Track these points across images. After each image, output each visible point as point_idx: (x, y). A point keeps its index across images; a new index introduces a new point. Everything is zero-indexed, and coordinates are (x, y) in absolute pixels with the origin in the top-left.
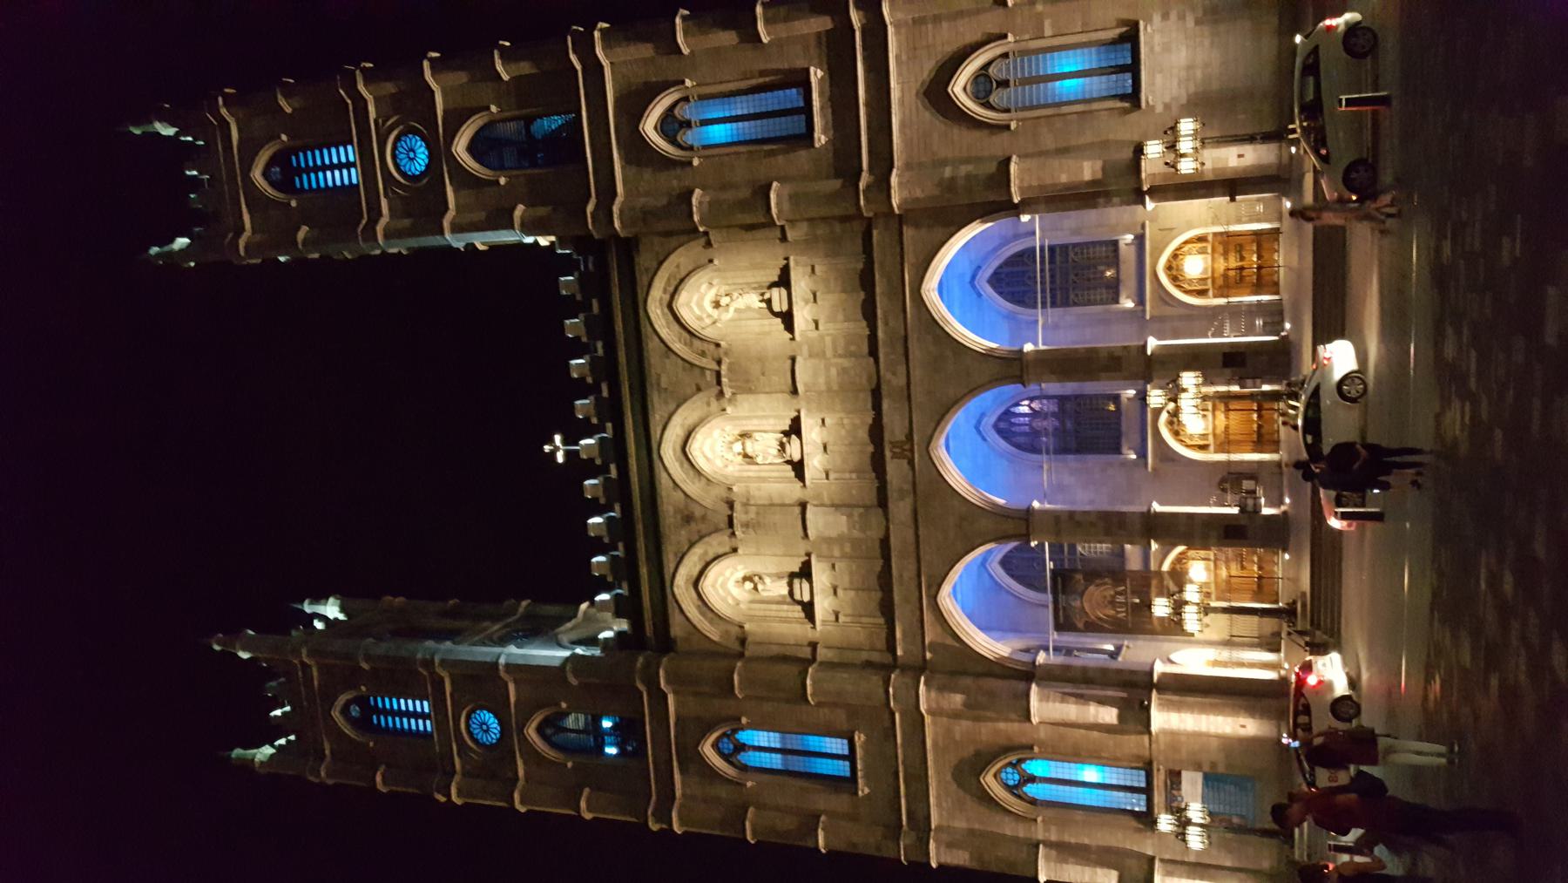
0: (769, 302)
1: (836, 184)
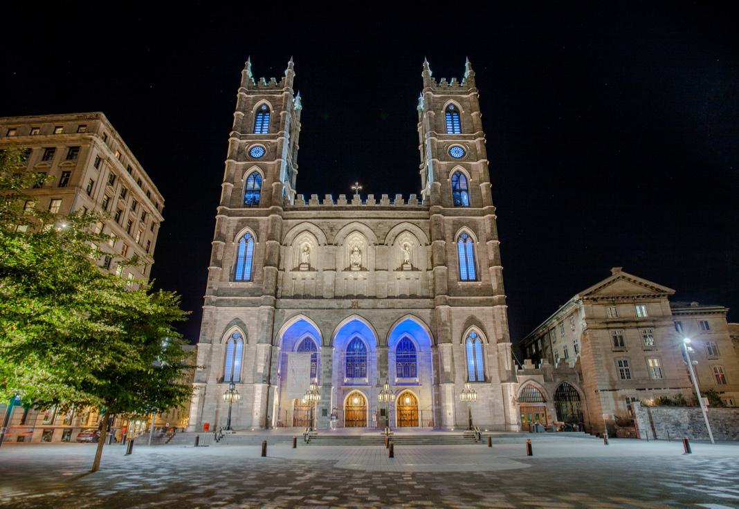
0: (407, 263)
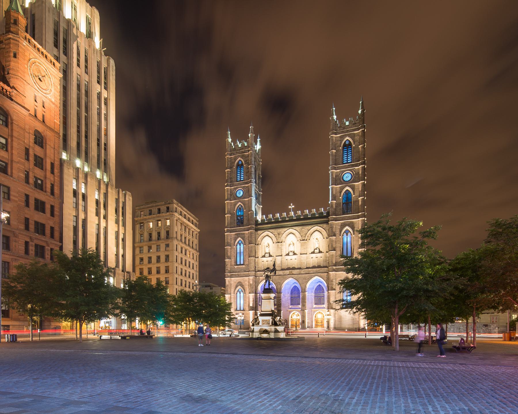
1: (334, 262)
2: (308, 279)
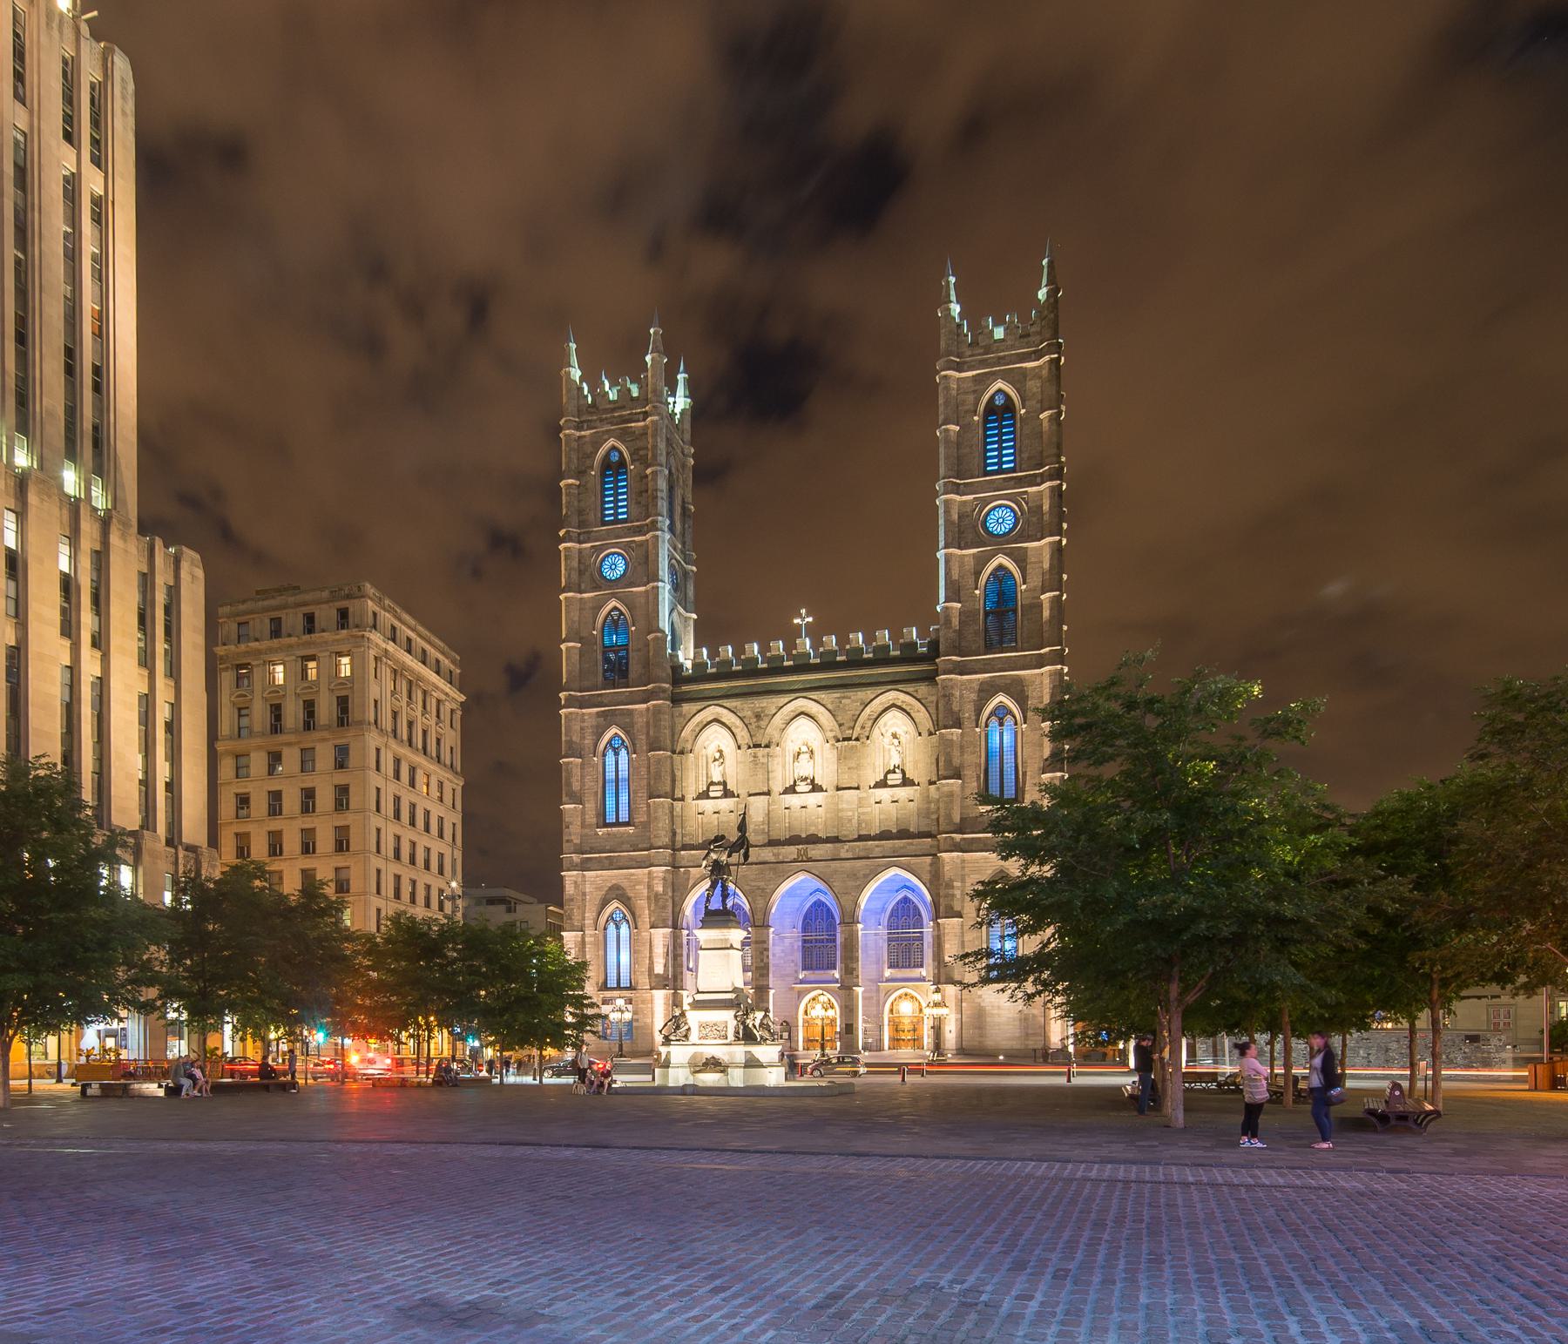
0: (895, 772)
1: (957, 819)
2: (866, 876)
